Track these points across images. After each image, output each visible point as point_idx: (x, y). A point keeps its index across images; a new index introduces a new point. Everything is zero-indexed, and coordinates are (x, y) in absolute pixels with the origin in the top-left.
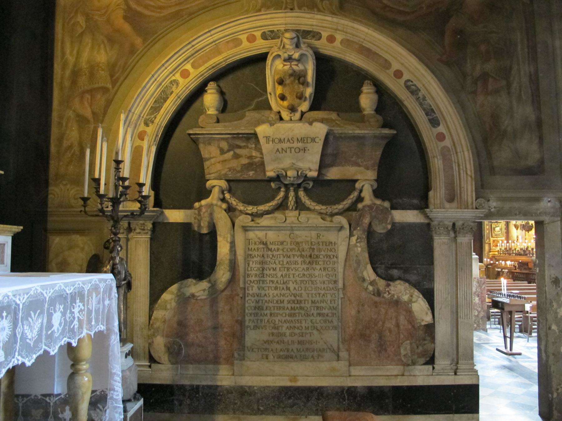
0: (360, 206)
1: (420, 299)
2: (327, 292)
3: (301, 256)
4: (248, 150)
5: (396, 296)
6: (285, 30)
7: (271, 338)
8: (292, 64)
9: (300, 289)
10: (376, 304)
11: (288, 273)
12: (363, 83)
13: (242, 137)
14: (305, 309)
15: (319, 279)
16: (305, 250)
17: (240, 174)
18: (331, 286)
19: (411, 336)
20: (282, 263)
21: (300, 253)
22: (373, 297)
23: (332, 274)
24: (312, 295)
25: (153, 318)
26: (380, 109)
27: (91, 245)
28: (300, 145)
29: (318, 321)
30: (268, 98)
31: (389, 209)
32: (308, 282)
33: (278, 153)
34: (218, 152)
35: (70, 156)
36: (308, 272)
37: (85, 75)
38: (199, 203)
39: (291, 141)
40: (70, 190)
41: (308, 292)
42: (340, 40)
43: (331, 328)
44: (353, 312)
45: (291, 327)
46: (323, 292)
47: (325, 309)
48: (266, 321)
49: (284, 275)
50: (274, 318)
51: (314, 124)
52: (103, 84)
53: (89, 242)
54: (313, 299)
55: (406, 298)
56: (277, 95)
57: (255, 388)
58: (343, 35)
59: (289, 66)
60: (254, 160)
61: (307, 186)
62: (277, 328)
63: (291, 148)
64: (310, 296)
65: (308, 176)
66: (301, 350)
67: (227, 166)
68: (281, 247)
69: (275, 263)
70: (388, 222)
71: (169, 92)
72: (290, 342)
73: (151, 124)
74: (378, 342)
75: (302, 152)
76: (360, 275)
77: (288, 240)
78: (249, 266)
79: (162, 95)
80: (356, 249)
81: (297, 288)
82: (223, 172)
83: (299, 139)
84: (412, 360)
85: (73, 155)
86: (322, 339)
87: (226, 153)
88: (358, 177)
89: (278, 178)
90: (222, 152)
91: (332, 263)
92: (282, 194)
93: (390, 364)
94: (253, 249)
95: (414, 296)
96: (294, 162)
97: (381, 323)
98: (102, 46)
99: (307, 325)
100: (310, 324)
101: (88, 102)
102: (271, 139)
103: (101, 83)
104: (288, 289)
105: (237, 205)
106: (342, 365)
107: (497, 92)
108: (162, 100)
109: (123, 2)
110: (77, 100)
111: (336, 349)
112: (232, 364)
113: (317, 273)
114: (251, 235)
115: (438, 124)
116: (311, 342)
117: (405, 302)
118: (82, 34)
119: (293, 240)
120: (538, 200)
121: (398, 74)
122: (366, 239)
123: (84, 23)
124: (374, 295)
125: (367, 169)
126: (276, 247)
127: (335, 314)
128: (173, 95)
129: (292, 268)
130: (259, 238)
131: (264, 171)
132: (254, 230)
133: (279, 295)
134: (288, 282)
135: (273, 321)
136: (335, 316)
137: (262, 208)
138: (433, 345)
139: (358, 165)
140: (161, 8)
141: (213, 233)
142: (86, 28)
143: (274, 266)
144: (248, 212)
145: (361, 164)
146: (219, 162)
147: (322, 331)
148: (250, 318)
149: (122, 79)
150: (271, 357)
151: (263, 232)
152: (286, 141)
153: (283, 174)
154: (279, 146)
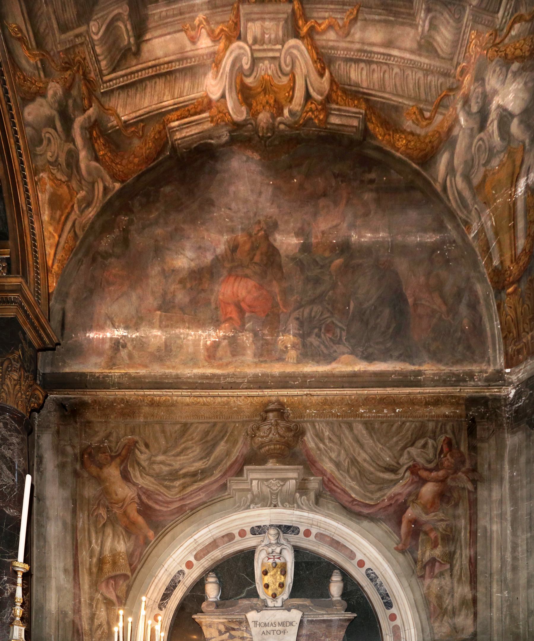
4: (240, 632)
12: (332, 572)
26: (344, 595)
28: (281, 628)
51: (292, 610)
71: (177, 581)
85: (103, 632)
87: (223, 634)
90: (221, 633)
98: (121, 537)
107: (442, 574)
110: (103, 585)
115: (391, 607)
118: (104, 525)
121: (361, 564)
140: (168, 503)
149: (139, 567)
154: (265, 629)
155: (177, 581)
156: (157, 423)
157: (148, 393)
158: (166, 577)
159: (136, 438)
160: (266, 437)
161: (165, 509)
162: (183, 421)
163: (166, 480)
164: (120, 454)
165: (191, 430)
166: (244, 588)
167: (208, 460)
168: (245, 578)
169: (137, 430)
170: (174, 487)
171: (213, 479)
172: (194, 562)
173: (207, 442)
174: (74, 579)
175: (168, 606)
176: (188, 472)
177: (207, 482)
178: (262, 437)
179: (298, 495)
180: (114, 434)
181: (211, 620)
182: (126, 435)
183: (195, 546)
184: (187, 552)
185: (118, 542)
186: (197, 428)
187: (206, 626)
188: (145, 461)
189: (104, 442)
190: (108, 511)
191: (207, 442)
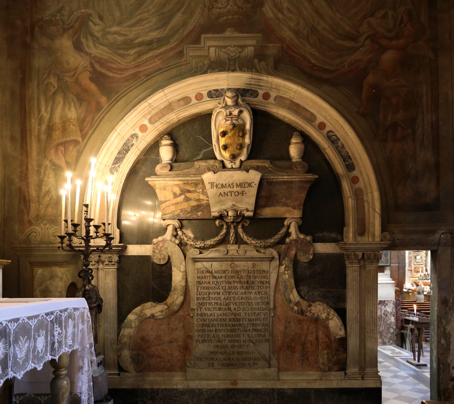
0: (287, 240)
1: (335, 317)
2: (260, 312)
3: (240, 282)
5: (316, 315)
6: (227, 89)
7: (216, 350)
8: (233, 119)
9: (239, 309)
10: (300, 322)
11: (229, 296)
13: (192, 183)
14: (243, 325)
15: (254, 301)
16: (243, 277)
17: (190, 214)
18: (264, 306)
19: (328, 347)
20: (224, 288)
21: (239, 280)
22: (298, 315)
23: (265, 297)
24: (249, 314)
25: (120, 335)
27: (68, 275)
28: (239, 189)
29: (253, 336)
30: (213, 149)
31: (312, 242)
32: (245, 303)
33: (221, 196)
34: (172, 196)
35: (48, 199)
36: (245, 296)
37: (59, 129)
38: (157, 239)
39: (232, 186)
40: (49, 228)
41: (245, 312)
42: (274, 97)
43: (264, 341)
44: (282, 328)
45: (232, 340)
46: (257, 312)
47: (258, 320)
48: (212, 336)
49: (226, 298)
50: (218, 333)
51: (250, 171)
52: (74, 138)
53: (66, 273)
54: (250, 318)
55: (324, 316)
56: (221, 146)
57: (204, 390)
58: (277, 92)
59: (230, 121)
60: (202, 202)
61: (245, 224)
62: (221, 342)
63: (231, 192)
64: (247, 315)
65: (245, 215)
66: (240, 359)
67: (180, 208)
68: (223, 275)
69: (219, 288)
70: (311, 253)
71: (130, 145)
72: (231, 353)
74: (302, 352)
75: (240, 195)
76: (287, 297)
77: (230, 269)
78: (198, 291)
79: (124, 147)
80: (284, 275)
81: (236, 309)
82: (176, 213)
83: (238, 184)
84: (329, 367)
86: (257, 350)
87: (178, 197)
88: (287, 215)
89: (221, 217)
90: (175, 196)
91: (264, 287)
92: (224, 231)
93: (311, 371)
94: (201, 277)
95: (330, 314)
96: (234, 204)
97: (303, 337)
98: (72, 104)
99: (244, 339)
100: (248, 338)
101: (62, 153)
102: (215, 185)
103: (73, 137)
104: (229, 309)
105: (188, 240)
106: (273, 371)
108: (124, 152)
109: (90, 65)
111: (267, 357)
112: (185, 371)
113: (253, 296)
114: (199, 265)
115: (354, 169)
116: (248, 353)
117: (323, 319)
118: (55, 93)
119: (234, 269)
120: (433, 232)
121: (322, 126)
122: (292, 268)
123: (56, 83)
124: (298, 313)
125: (294, 208)
126: (220, 275)
127: (267, 329)
129: (233, 292)
130: (206, 268)
131: (210, 212)
132: (202, 261)
133: (222, 315)
134: (229, 304)
135: (218, 336)
136: (267, 331)
137: (208, 242)
138: (345, 355)
139: (286, 205)
140: (121, 70)
141: (168, 265)
142: (58, 87)
143: (218, 291)
144: (196, 246)
145: (289, 204)
146: (173, 205)
147: (256, 343)
148: (199, 333)
150: (216, 365)
151: (209, 262)
152: (227, 186)
153: (225, 214)
154: (222, 190)
155: (130, 145)
159: (90, 11)
160: (224, 8)
161: (118, 76)
163: (121, 48)
164: (72, 27)
166: (200, 150)
167: (164, 30)
168: (202, 140)
170: (128, 55)
171: (168, 47)
172: (149, 125)
174: (22, 147)
175: (120, 170)
176: (143, 41)
177: (163, 49)
178: (220, 8)
179: (256, 61)
180: (67, 9)
181: (164, 182)
182: (79, 8)
183: (150, 109)
184: (141, 117)
185: (69, 109)
187: (160, 188)
188: (99, 32)
189: (55, 16)
190: (59, 80)
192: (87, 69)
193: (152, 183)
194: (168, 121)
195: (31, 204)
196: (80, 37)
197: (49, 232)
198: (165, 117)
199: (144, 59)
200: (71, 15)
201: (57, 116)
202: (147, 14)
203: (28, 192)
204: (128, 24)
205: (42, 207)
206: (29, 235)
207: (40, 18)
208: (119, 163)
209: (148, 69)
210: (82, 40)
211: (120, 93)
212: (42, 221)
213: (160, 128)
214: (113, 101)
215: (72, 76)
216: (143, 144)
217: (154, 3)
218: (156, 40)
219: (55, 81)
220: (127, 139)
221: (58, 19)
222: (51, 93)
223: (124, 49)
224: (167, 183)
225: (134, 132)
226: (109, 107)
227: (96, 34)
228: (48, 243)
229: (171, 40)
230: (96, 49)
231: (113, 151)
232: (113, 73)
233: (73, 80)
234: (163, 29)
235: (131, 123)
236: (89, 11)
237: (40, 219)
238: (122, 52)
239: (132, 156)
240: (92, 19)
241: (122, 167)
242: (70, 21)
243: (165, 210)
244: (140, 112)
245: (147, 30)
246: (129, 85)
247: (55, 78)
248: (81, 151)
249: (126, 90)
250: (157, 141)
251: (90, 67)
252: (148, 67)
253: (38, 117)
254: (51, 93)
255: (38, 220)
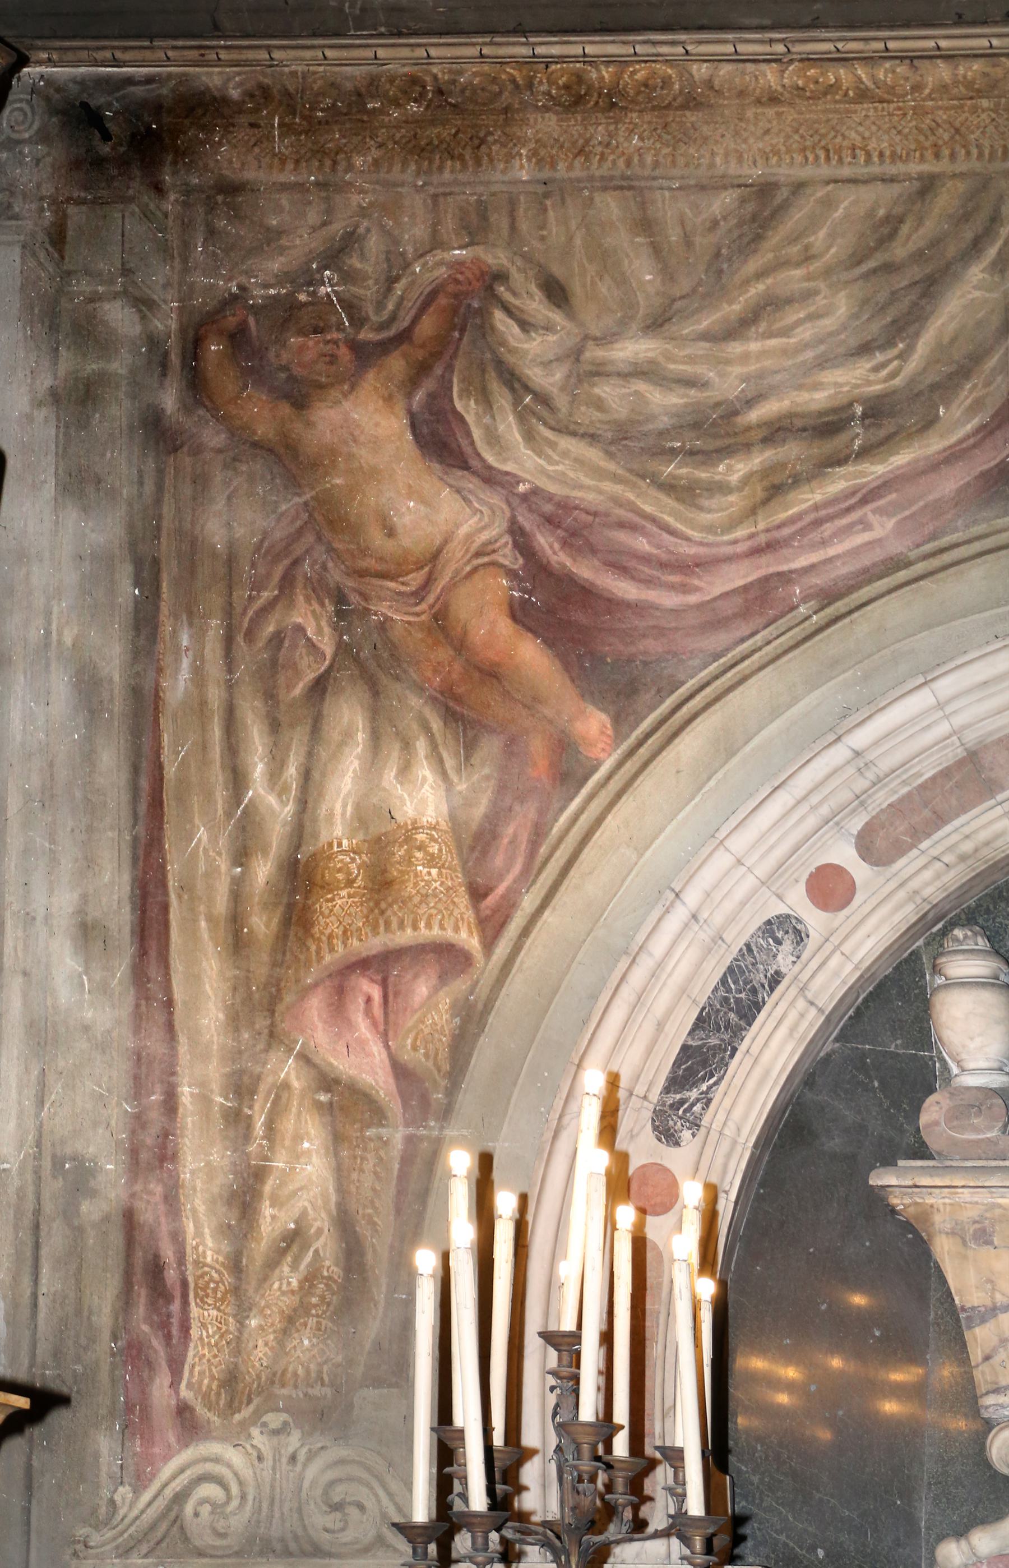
35: (295, 1283)
37: (350, 883)
40: (302, 1456)
52: (436, 931)
71: (759, 977)
73: (686, 1134)
79: (729, 990)
85: (310, 1280)
98: (421, 746)
101: (368, 1012)
103: (429, 926)
108: (732, 1015)
109: (507, 538)
110: (315, 1006)
118: (320, 687)
123: (327, 630)
128: (780, 988)
142: (336, 655)
149: (528, 902)
155: (759, 977)
156: (608, 185)
157: (555, 50)
158: (693, 955)
159: (496, 258)
161: (670, 600)
162: (756, 173)
163: (673, 452)
164: (404, 337)
165: (797, 217)
167: (902, 356)
169: (500, 221)
170: (722, 488)
171: (934, 444)
172: (859, 870)
173: (888, 268)
174: (139, 976)
175: (714, 1118)
176: (791, 415)
177: (901, 459)
180: (374, 244)
181: (984, 1197)
182: (436, 243)
183: (861, 784)
184: (812, 822)
185: (405, 770)
186: (828, 203)
187: (957, 1233)
188: (546, 364)
189: (313, 281)
190: (340, 614)
191: (888, 268)
192: (494, 557)
193: (907, 1201)
194: (967, 847)
195: (195, 1311)
196: (451, 389)
197: (301, 1478)
198: (948, 828)
199: (804, 506)
200: (397, 279)
201: (338, 809)
202: (798, 273)
203: (177, 1237)
204: (705, 323)
205: (261, 1328)
206: (180, 1498)
207: (234, 289)
208: (703, 1079)
209: (830, 560)
210: (459, 405)
211: (683, 691)
212: (257, 1414)
213: (927, 884)
214: (648, 736)
215: (414, 594)
216: (836, 974)
217: (836, 215)
218: (859, 410)
219: (324, 623)
220: (741, 943)
221: (328, 295)
222: (301, 685)
223: (692, 453)
224: (1000, 1206)
225: (782, 909)
226: (630, 767)
227: (536, 376)
228: (293, 1546)
229: (942, 411)
230: (540, 454)
231: (669, 1013)
232: (640, 581)
233: (417, 614)
234: (895, 352)
235: (763, 857)
236: (490, 260)
237: (249, 1402)
238: (684, 471)
239: (774, 1043)
240: (508, 297)
241: (727, 1102)
242: (390, 306)
243: (996, 1360)
244: (805, 798)
245: (809, 355)
246: (728, 650)
247: (322, 605)
248: (480, 1006)
249: (716, 677)
250: (906, 960)
251: (508, 550)
252: (831, 552)
253: (229, 815)
254: (301, 685)
255: (232, 1408)
